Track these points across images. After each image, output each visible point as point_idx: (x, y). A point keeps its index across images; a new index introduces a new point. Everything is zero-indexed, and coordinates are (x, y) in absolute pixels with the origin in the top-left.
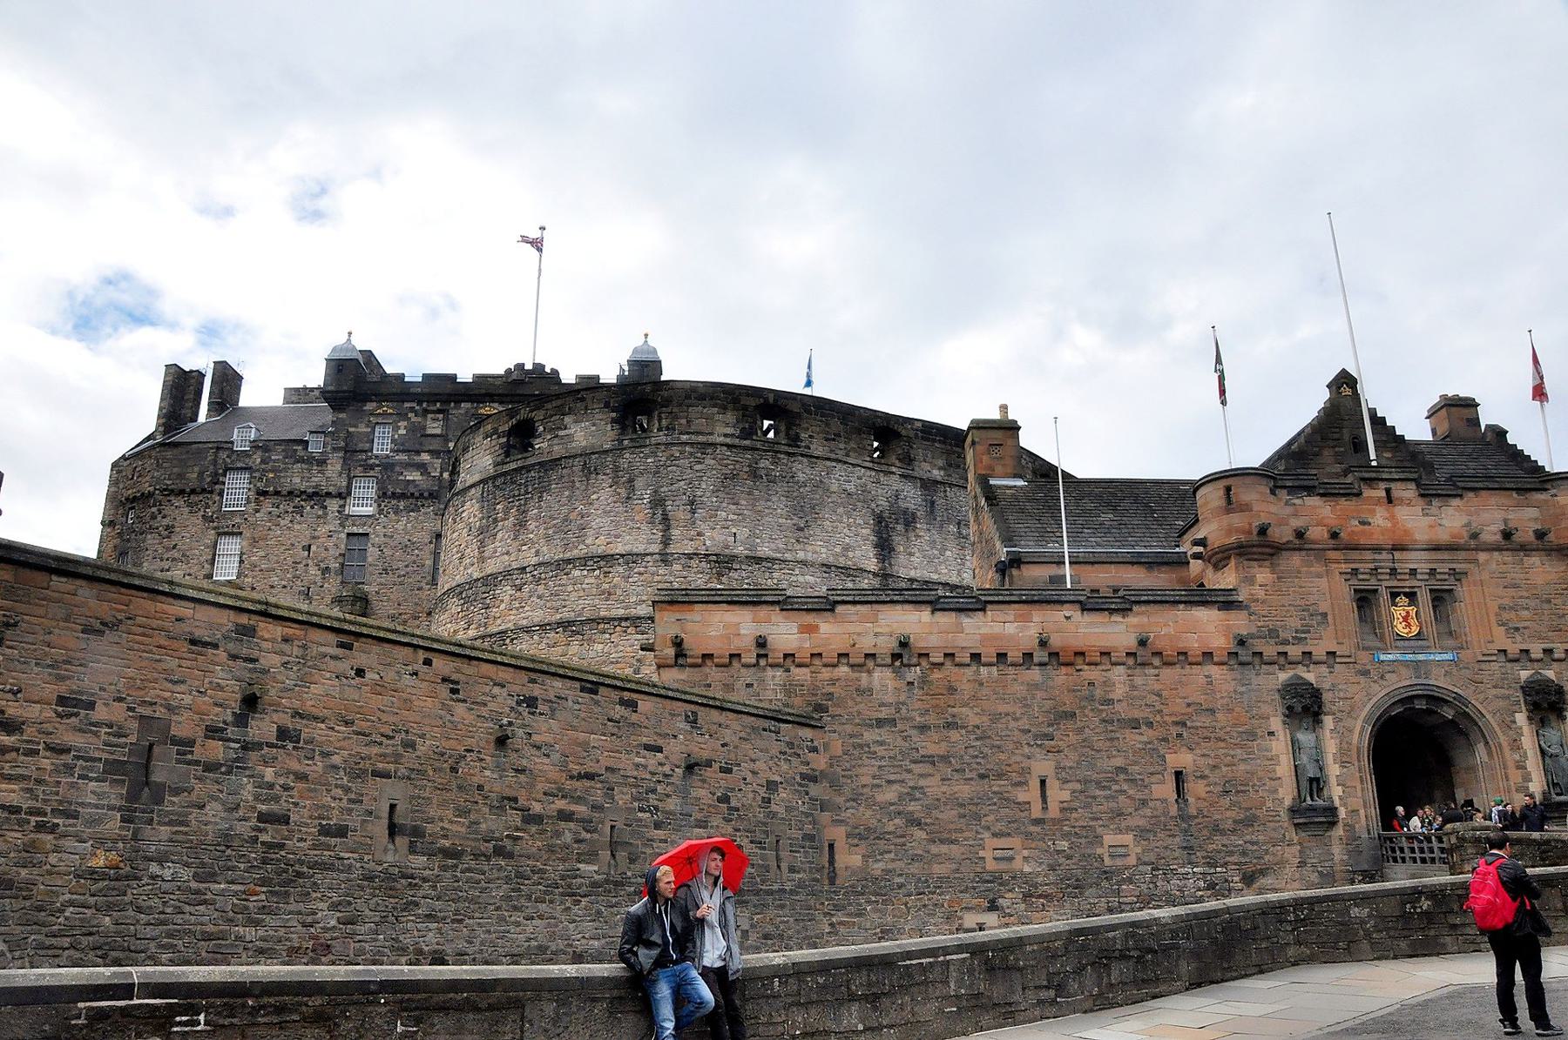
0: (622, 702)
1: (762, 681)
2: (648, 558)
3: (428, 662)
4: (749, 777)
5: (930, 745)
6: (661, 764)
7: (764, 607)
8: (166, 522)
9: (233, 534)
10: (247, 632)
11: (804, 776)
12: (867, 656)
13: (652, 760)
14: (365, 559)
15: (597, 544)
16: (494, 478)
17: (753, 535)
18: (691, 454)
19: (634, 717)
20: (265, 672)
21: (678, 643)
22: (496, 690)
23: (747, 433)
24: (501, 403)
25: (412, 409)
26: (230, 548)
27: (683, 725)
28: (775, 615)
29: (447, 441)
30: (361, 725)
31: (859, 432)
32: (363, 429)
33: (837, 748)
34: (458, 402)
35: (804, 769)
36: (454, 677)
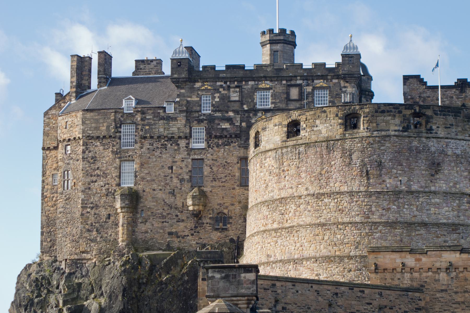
0: (360, 291)
1: (403, 277)
2: (360, 194)
3: (312, 287)
4: (398, 310)
5: (459, 298)
6: (372, 308)
7: (404, 253)
8: (90, 155)
9: (129, 160)
10: (274, 285)
11: (416, 309)
12: (438, 269)
13: (369, 307)
14: (203, 173)
15: (335, 186)
16: (282, 148)
17: (409, 180)
18: (379, 142)
19: (364, 295)
20: (278, 294)
21: (376, 265)
22: (328, 292)
23: (406, 129)
24: (271, 81)
25: (221, 86)
26: (129, 168)
27: (378, 296)
28: (408, 256)
29: (242, 104)
30: (299, 304)
31: (464, 121)
32: (195, 99)
33: (428, 299)
34: (247, 81)
35: (416, 306)
36: (318, 290)
